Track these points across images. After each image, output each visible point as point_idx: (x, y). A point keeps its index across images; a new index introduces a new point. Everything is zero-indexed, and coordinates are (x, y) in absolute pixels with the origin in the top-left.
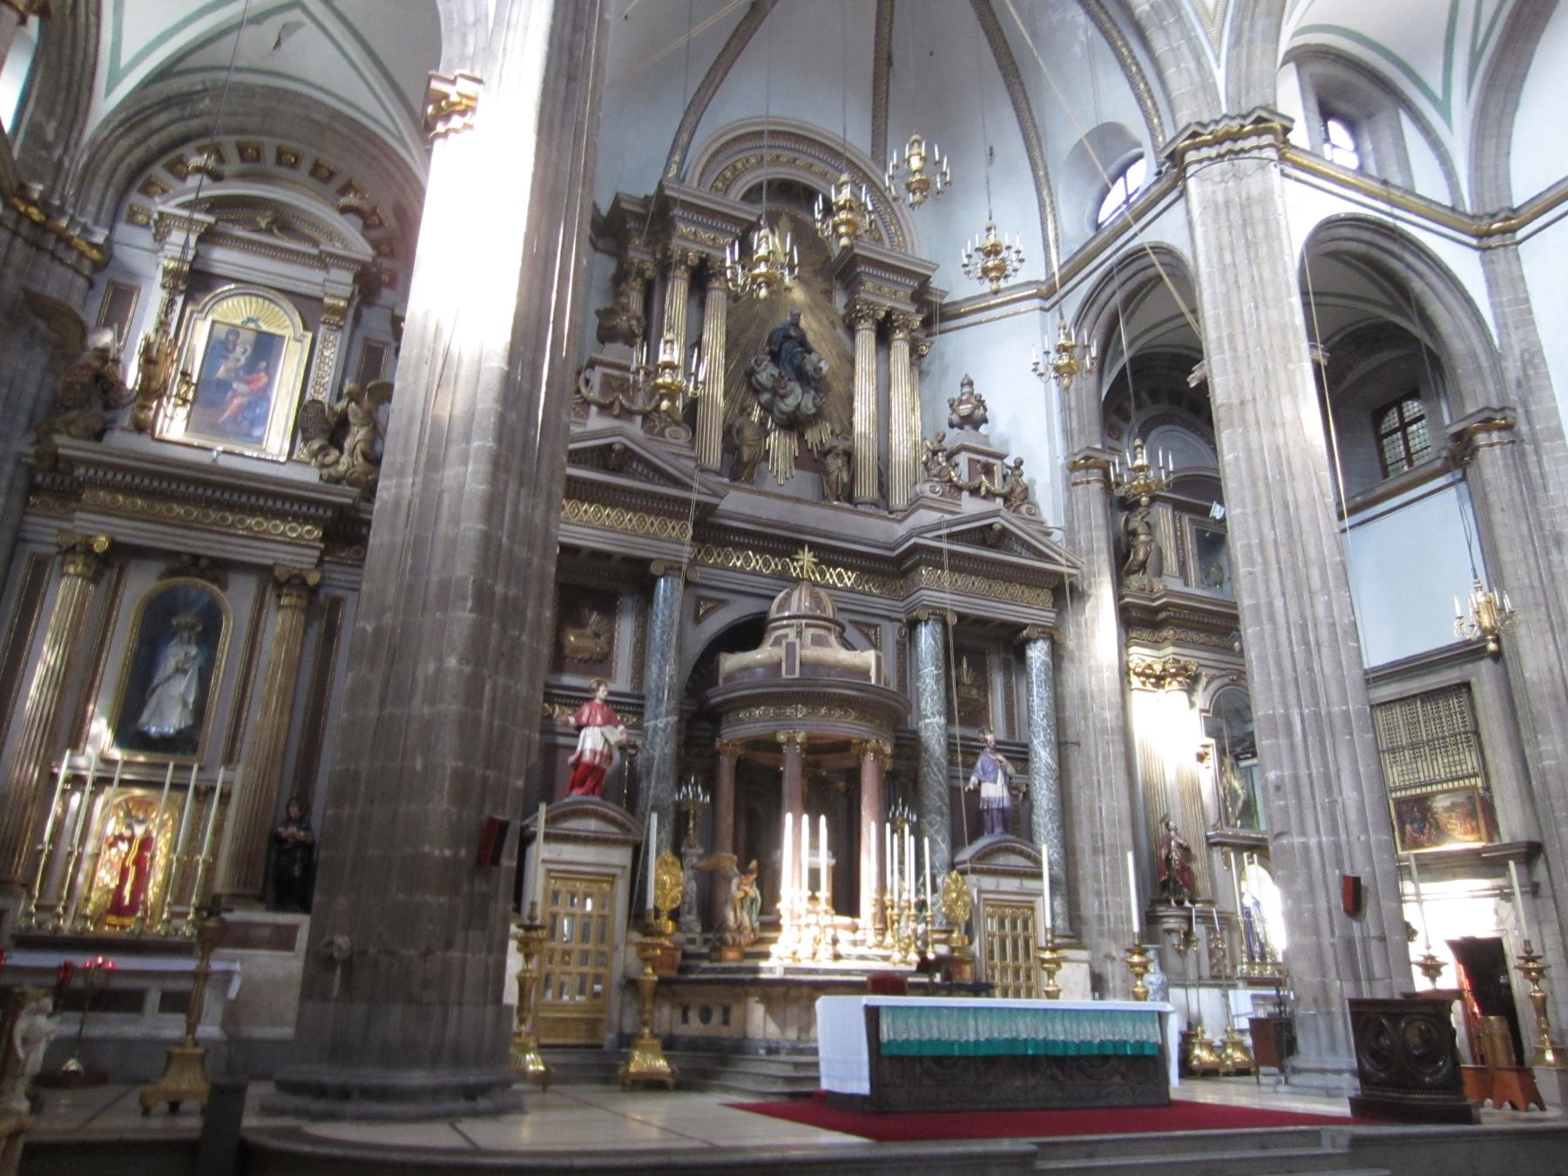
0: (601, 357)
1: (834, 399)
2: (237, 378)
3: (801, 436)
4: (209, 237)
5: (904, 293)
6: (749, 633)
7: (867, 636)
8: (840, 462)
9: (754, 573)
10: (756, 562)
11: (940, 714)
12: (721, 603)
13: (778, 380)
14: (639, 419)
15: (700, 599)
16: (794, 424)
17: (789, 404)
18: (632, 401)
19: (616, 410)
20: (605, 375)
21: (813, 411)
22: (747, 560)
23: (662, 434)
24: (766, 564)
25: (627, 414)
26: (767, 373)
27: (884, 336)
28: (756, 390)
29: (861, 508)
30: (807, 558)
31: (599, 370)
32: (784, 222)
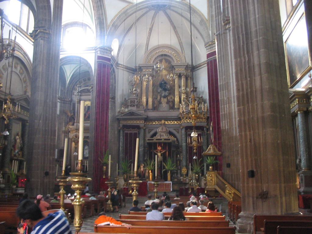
0: (129, 98)
1: (171, 91)
2: (87, 113)
3: (167, 98)
4: (80, 96)
5: (183, 69)
6: (155, 134)
7: (176, 131)
8: (171, 103)
9: (157, 124)
10: (157, 123)
11: (184, 143)
12: (152, 130)
13: (160, 91)
14: (136, 106)
15: (149, 130)
16: (165, 97)
17: (163, 95)
18: (135, 103)
19: (132, 106)
20: (131, 101)
21: (168, 94)
22: (156, 123)
23: (139, 107)
24: (159, 123)
25: (134, 106)
26: (160, 90)
27: (180, 76)
28: (159, 93)
29: (175, 110)
30: (163, 122)
31: (129, 100)
32: (164, 61)
